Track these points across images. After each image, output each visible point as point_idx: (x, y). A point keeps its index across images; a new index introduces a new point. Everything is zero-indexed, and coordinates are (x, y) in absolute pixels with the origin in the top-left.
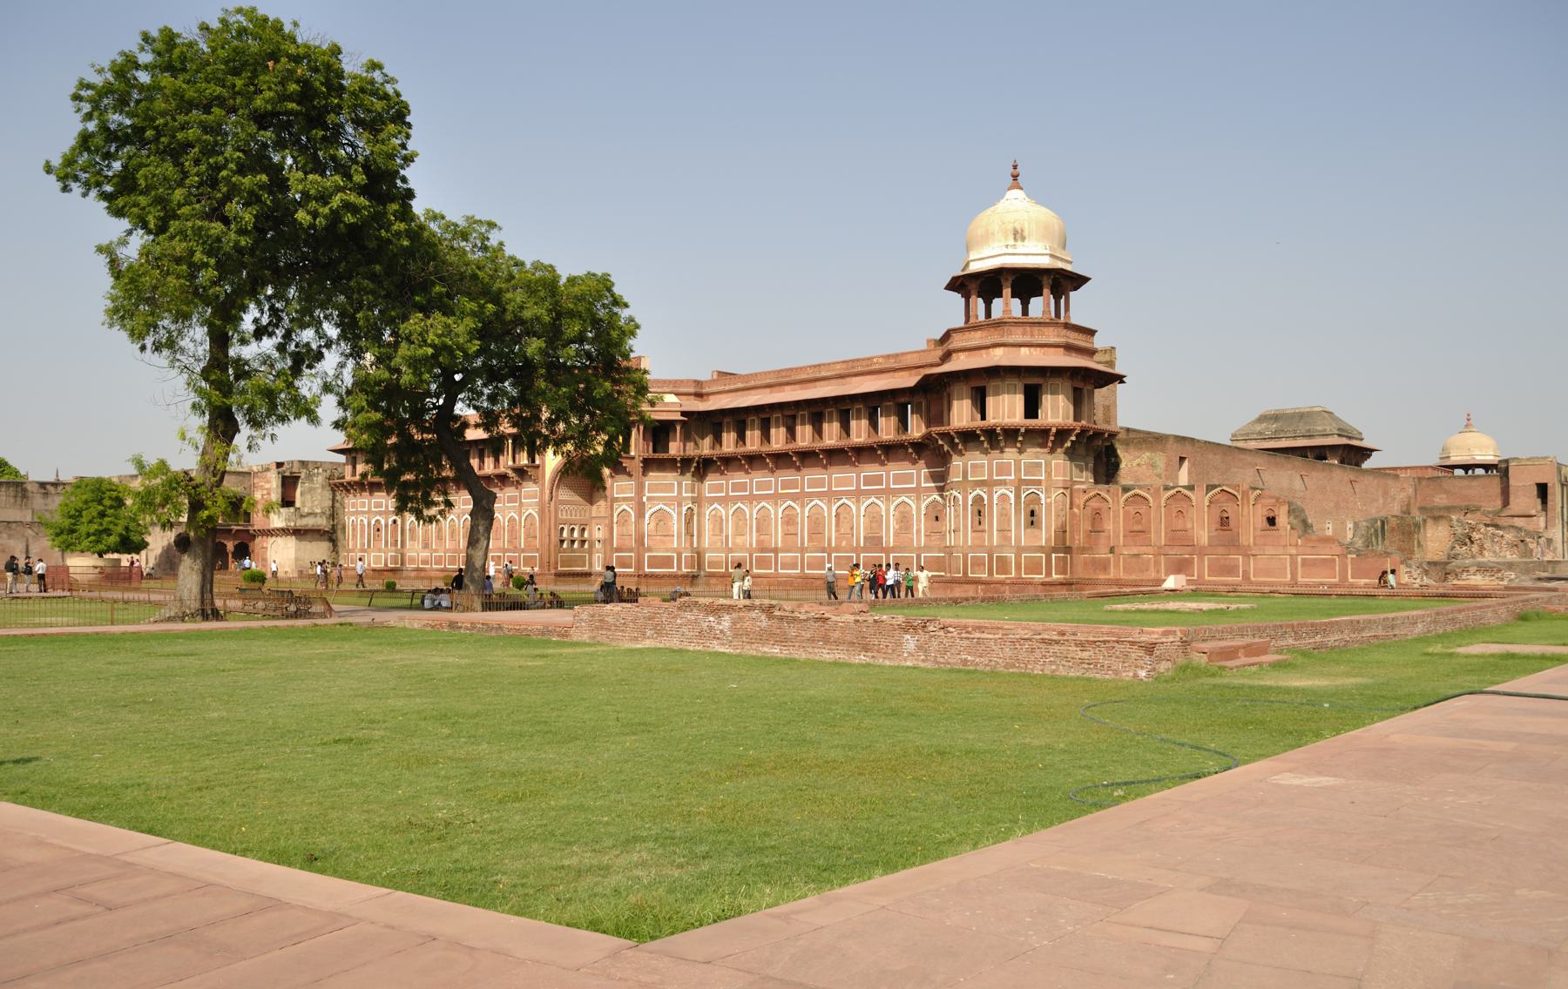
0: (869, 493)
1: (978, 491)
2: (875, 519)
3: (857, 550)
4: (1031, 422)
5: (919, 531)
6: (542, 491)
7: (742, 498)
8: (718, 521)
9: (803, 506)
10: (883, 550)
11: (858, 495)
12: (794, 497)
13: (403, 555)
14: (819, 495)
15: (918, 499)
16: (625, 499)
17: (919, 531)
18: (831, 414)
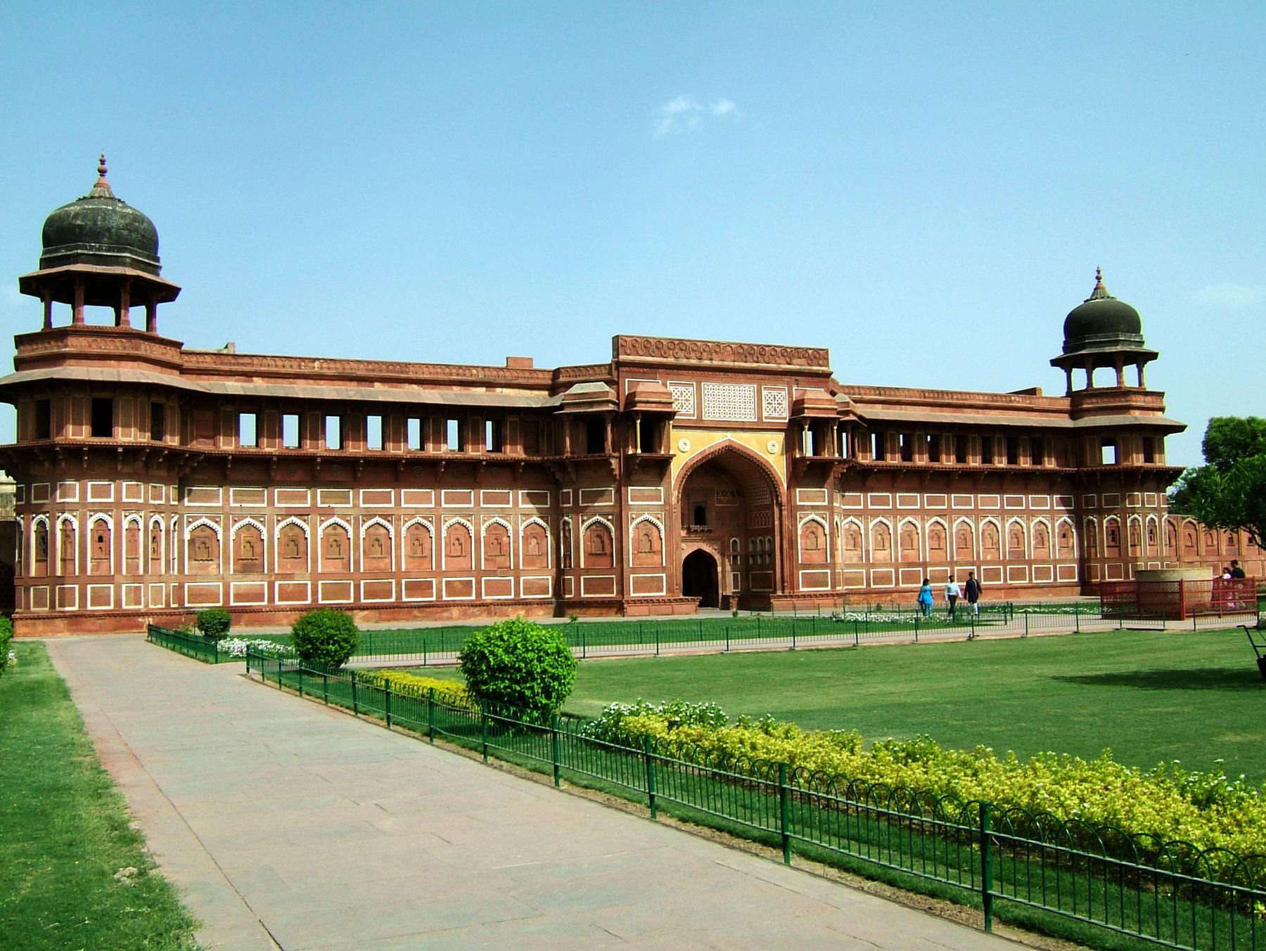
0: (1012, 513)
1: (1151, 516)
2: (1017, 537)
3: (1004, 563)
4: (1149, 465)
5: (1054, 546)
6: (668, 490)
7: (884, 513)
8: (855, 538)
9: (951, 522)
10: (1025, 562)
11: (1003, 514)
12: (941, 514)
13: (181, 587)
14: (967, 513)
15: (1053, 519)
16: (813, 508)
17: (1054, 546)
18: (974, 438)
